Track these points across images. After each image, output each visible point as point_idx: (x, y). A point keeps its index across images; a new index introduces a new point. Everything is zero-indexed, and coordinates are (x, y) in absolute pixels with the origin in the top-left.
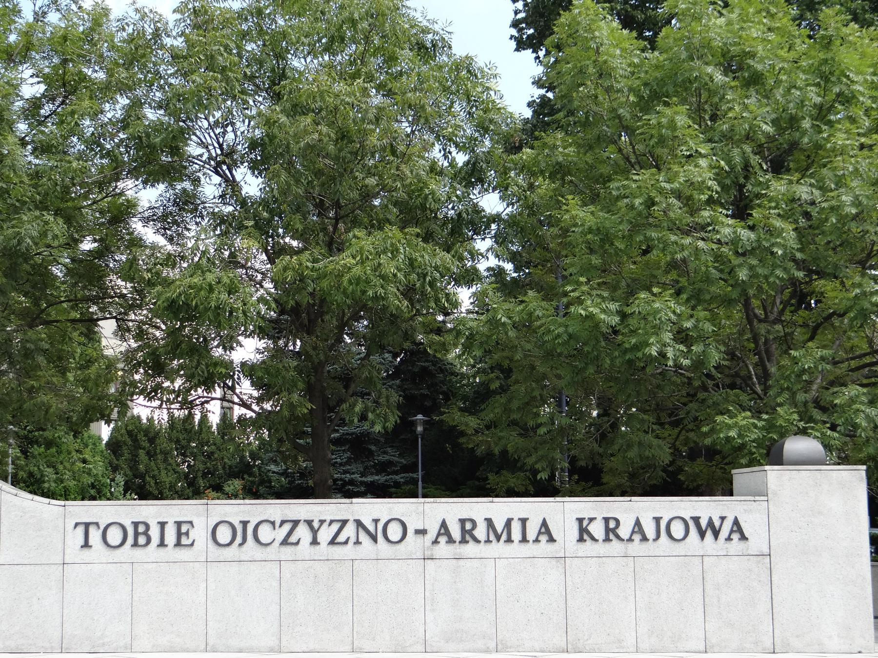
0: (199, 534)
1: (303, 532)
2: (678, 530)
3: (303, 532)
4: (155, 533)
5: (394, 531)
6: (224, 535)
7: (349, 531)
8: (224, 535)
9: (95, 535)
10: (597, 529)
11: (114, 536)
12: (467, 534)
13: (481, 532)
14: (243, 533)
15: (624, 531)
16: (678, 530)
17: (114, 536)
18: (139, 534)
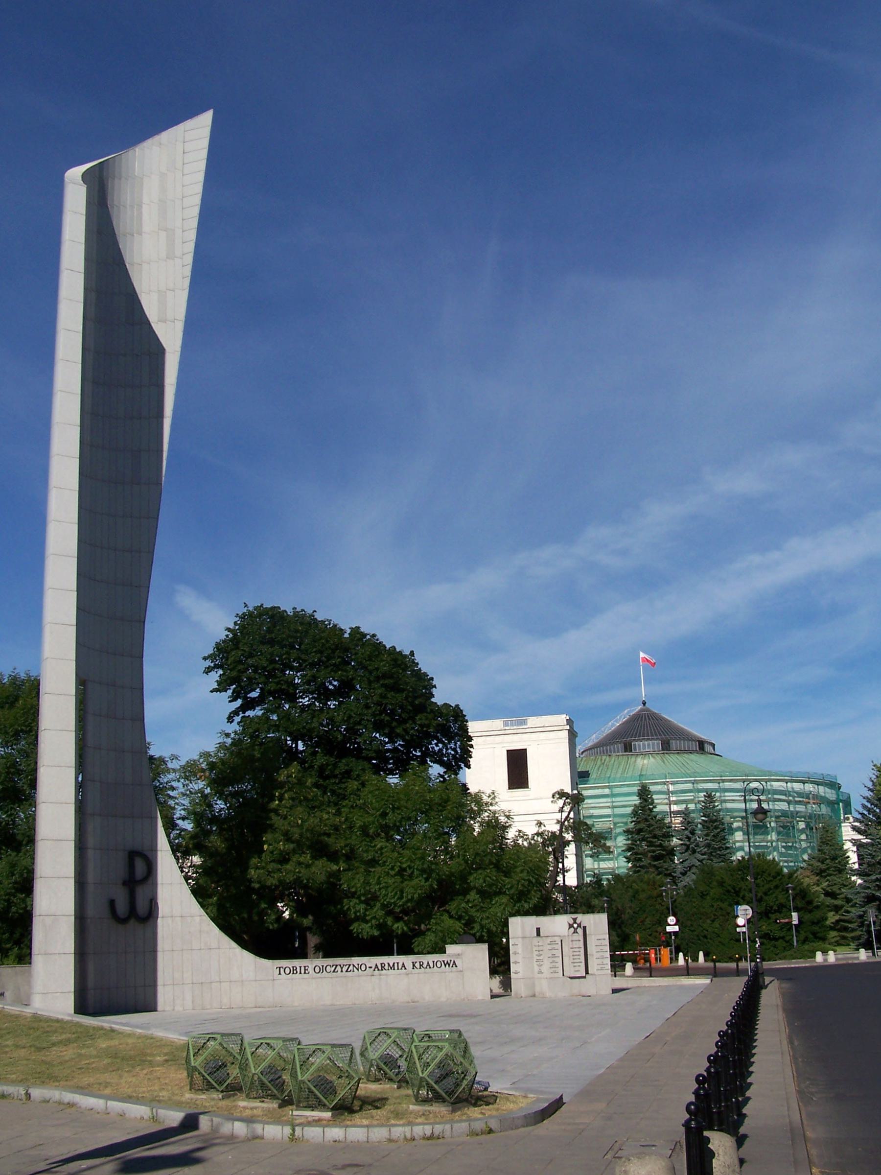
0: (311, 970)
1: (339, 968)
2: (439, 965)
3: (339, 968)
4: (298, 970)
5: (363, 968)
6: (317, 970)
7: (351, 967)
8: (317, 970)
9: (282, 970)
10: (417, 965)
11: (287, 971)
12: (383, 968)
13: (386, 967)
14: (323, 969)
15: (425, 966)
16: (439, 965)
17: (287, 971)
18: (294, 970)
